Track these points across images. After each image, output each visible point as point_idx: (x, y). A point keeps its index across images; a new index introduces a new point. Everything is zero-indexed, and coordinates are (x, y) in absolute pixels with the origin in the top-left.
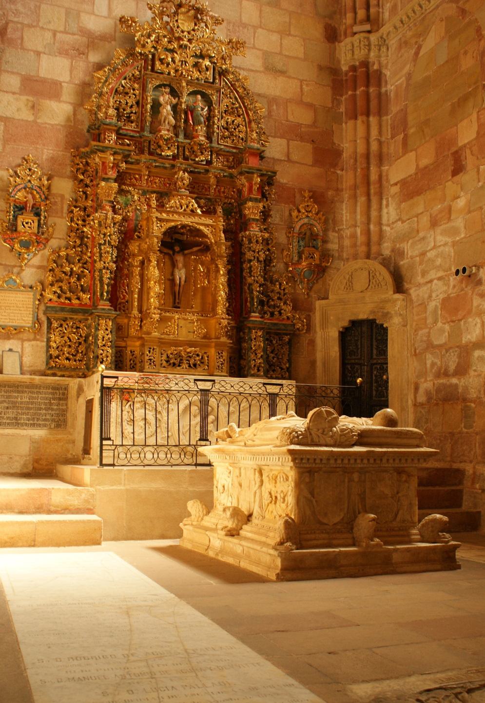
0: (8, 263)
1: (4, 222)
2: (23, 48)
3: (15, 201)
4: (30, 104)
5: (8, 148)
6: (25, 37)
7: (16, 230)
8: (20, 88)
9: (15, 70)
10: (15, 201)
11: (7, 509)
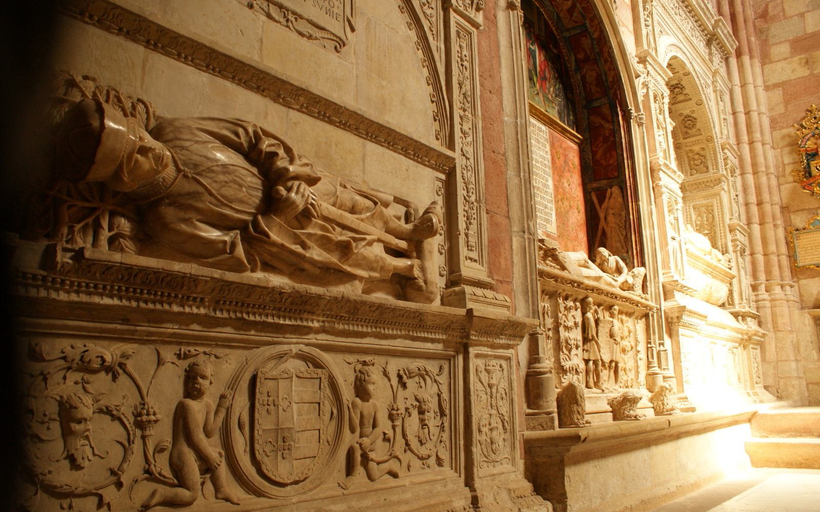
0: (811, 207)
1: (800, 171)
2: (786, 18)
3: (806, 150)
4: (804, 61)
5: (790, 107)
6: (786, 8)
7: (810, 176)
8: (791, 52)
9: (783, 40)
10: (806, 150)
11: (805, 432)
